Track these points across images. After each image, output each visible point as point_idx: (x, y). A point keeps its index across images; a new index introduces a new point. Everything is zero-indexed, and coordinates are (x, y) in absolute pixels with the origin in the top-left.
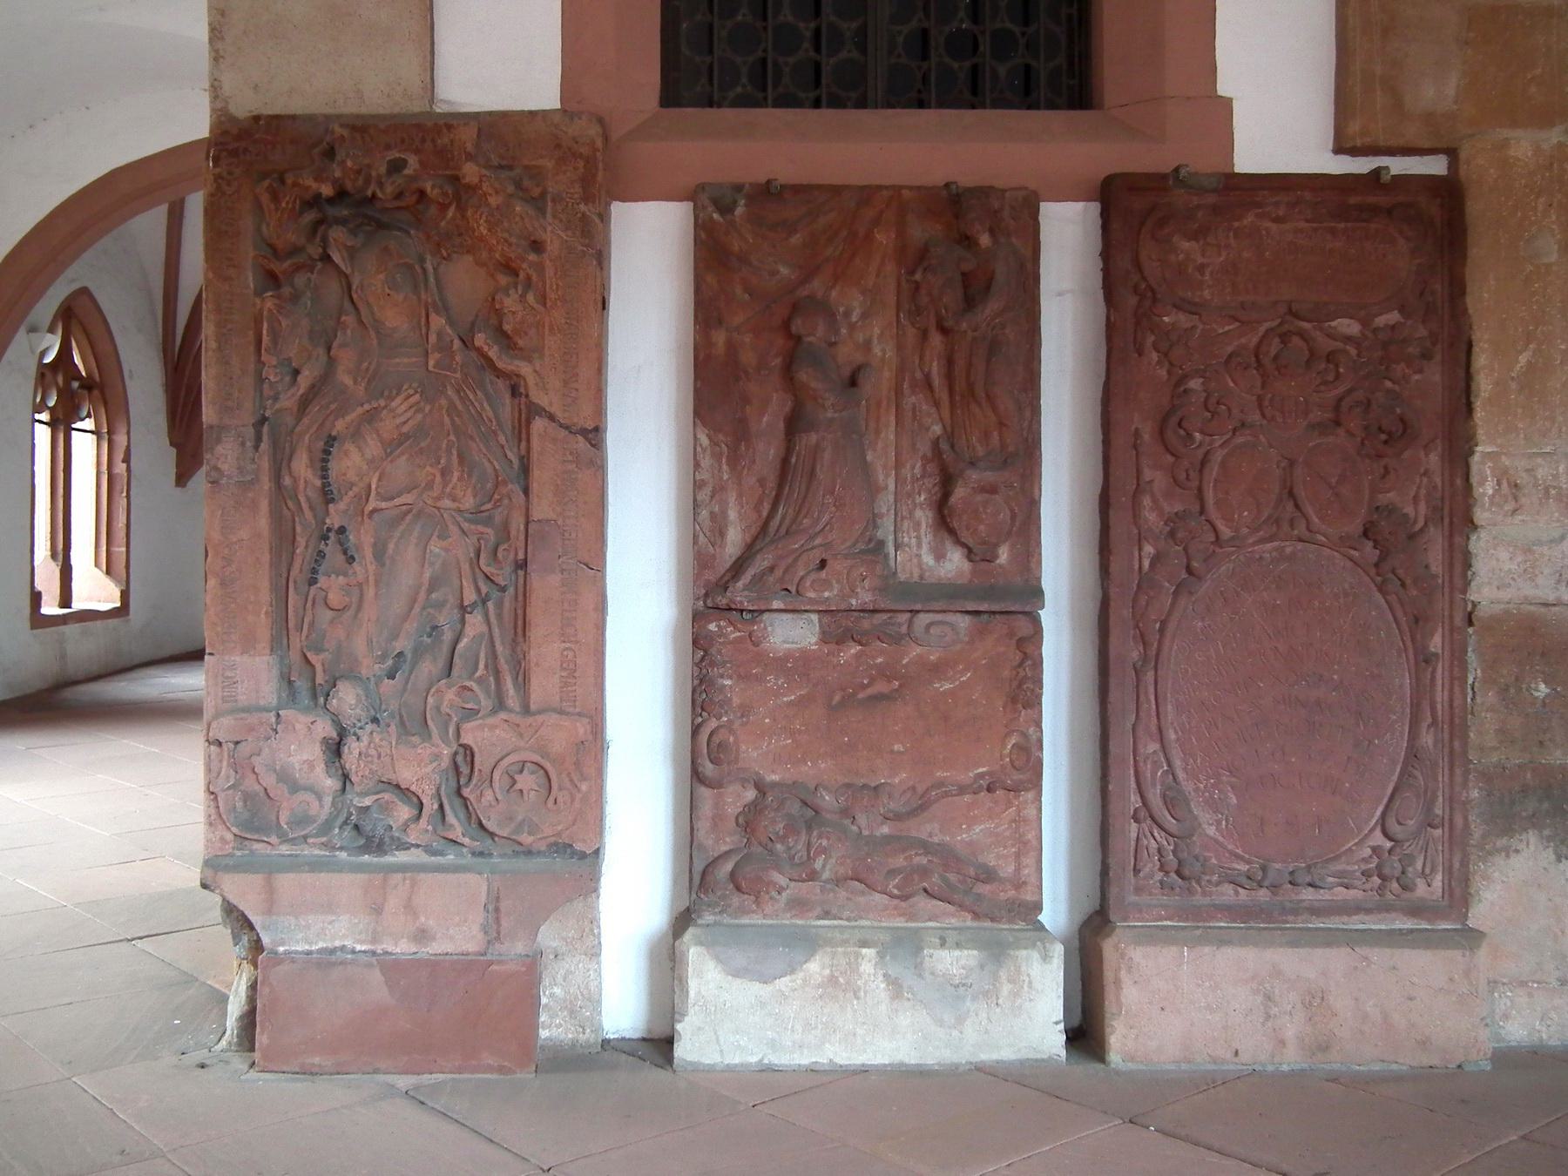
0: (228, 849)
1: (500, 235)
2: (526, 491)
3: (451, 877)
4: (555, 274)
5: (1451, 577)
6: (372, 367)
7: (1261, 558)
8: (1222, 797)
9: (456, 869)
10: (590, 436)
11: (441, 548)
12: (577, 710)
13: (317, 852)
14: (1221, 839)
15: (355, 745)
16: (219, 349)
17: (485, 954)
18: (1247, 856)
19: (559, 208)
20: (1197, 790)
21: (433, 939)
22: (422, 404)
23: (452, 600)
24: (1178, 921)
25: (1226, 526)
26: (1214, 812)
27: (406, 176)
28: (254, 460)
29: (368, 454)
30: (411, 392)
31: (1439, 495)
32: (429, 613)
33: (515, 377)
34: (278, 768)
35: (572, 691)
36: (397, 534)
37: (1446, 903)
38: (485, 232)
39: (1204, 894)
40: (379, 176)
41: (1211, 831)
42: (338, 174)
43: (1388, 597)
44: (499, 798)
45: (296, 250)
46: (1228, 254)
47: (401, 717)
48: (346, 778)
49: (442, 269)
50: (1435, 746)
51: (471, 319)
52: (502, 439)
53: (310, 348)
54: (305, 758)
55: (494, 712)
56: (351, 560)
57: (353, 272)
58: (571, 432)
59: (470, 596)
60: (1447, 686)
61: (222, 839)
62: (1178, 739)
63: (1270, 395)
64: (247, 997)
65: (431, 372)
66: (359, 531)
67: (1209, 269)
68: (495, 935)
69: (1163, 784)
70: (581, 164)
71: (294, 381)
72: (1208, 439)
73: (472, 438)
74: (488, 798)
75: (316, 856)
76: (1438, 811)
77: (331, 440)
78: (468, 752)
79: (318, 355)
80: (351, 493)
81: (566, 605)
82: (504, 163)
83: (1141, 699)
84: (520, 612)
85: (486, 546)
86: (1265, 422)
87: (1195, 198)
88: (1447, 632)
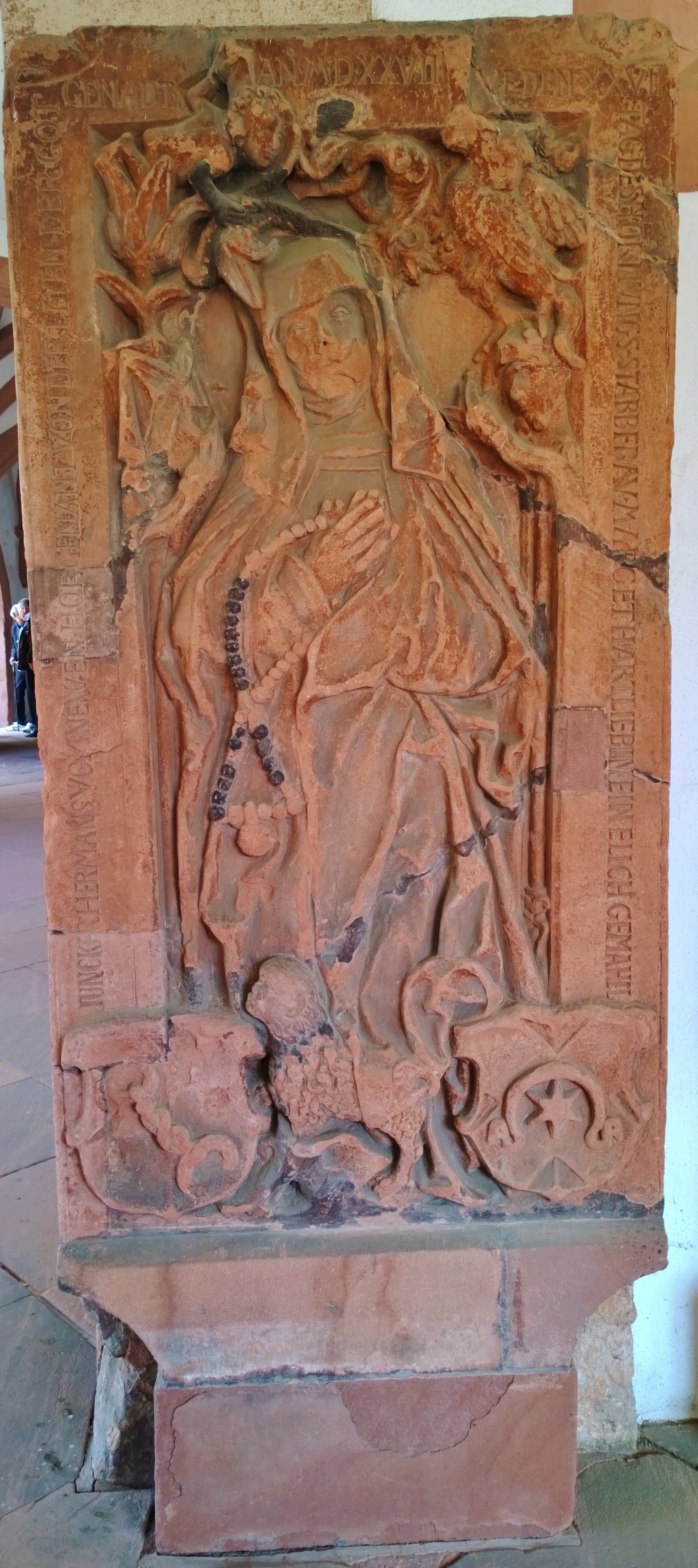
0: (98, 1227)
1: (510, 236)
2: (550, 661)
3: (444, 1255)
4: (601, 300)
6: (302, 465)
9: (454, 1242)
10: (655, 570)
11: (418, 755)
12: (633, 997)
13: (236, 1224)
15: (295, 1069)
16: (47, 439)
17: (501, 1367)
19: (608, 187)
21: (422, 1348)
22: (387, 525)
23: (436, 833)
27: (350, 134)
28: (114, 621)
29: (303, 609)
30: (370, 504)
32: (400, 857)
33: (529, 478)
34: (172, 1102)
35: (624, 970)
36: (351, 735)
38: (484, 232)
40: (306, 133)
42: (237, 128)
44: (516, 1132)
45: (165, 269)
47: (362, 1017)
48: (277, 1114)
49: (405, 298)
51: (456, 381)
52: (514, 577)
53: (196, 434)
54: (213, 1085)
55: (508, 1006)
56: (275, 779)
57: (264, 306)
58: (624, 565)
59: (464, 829)
61: (88, 1212)
64: (127, 1408)
65: (396, 471)
66: (288, 732)
68: (516, 1339)
70: (642, 109)
71: (175, 489)
73: (466, 577)
74: (500, 1136)
75: (238, 1230)
77: (240, 587)
78: (465, 1067)
79: (210, 447)
80: (274, 673)
81: (616, 840)
82: (515, 109)
84: (539, 848)
85: (487, 749)
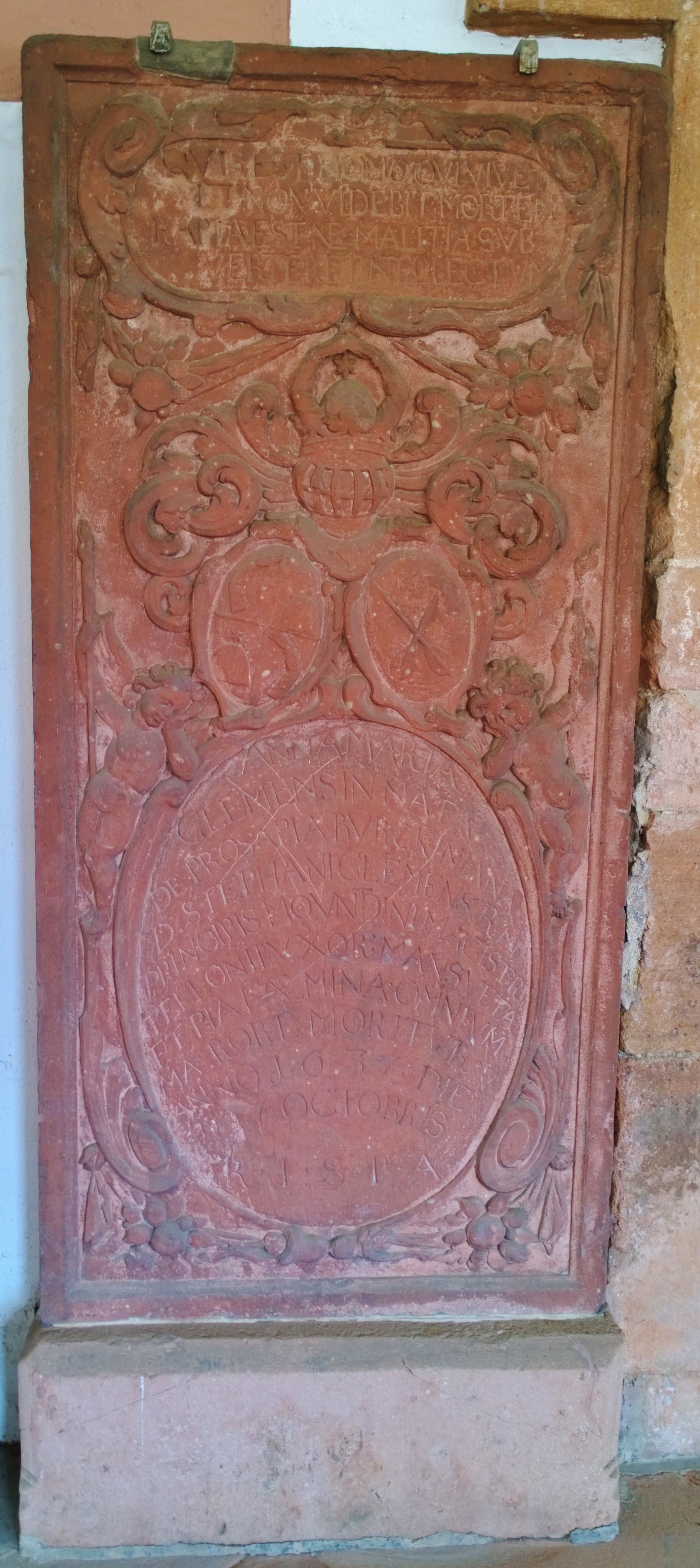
5: (606, 780)
7: (294, 747)
8: (222, 1130)
14: (220, 1191)
18: (263, 1217)
20: (183, 1119)
24: (152, 1317)
25: (234, 693)
26: (211, 1153)
31: (595, 644)
37: (572, 1278)
39: (197, 1272)
41: (206, 1181)
43: (500, 812)
46: (244, 204)
50: (565, 1044)
60: (590, 953)
62: (152, 1042)
63: (312, 467)
67: (211, 229)
69: (127, 1112)
72: (205, 543)
76: (567, 1143)
83: (91, 979)
86: (305, 515)
87: (188, 92)
88: (595, 870)
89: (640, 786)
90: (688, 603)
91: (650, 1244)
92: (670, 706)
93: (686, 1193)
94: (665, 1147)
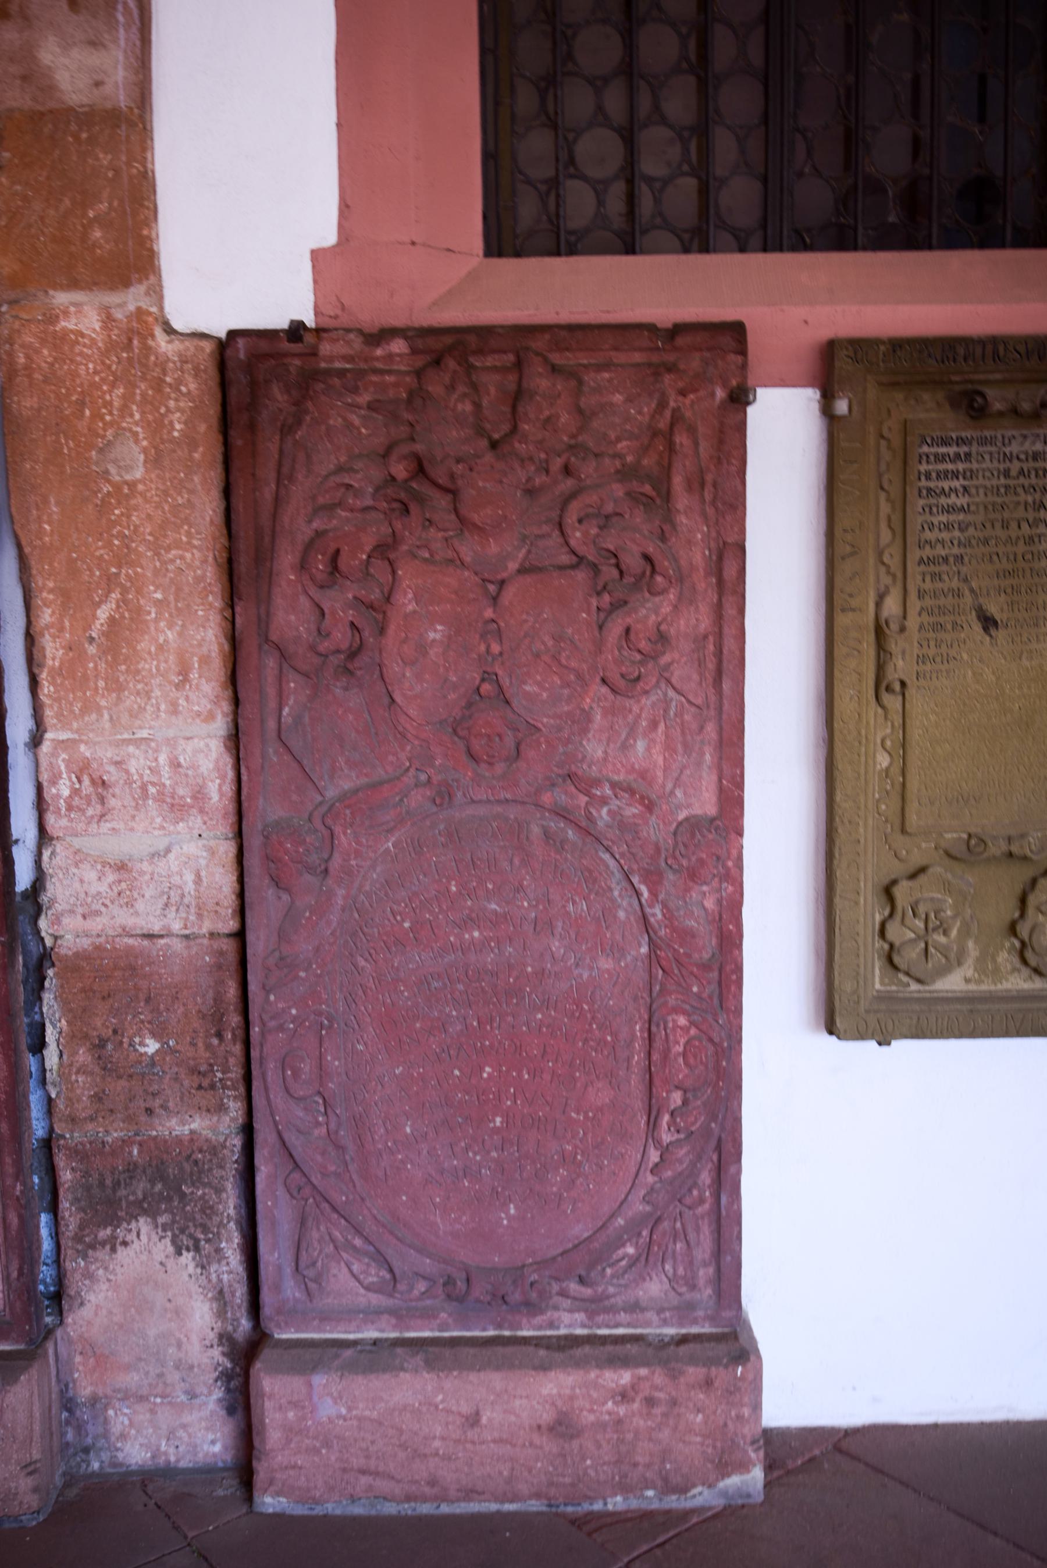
89: (43, 917)
90: (63, 768)
91: (94, 1291)
92: (58, 850)
93: (119, 1249)
94: (97, 1211)
